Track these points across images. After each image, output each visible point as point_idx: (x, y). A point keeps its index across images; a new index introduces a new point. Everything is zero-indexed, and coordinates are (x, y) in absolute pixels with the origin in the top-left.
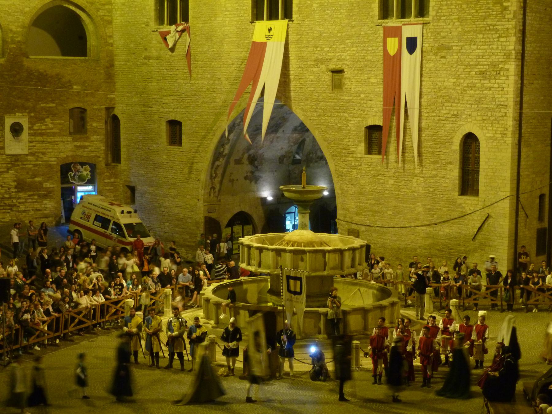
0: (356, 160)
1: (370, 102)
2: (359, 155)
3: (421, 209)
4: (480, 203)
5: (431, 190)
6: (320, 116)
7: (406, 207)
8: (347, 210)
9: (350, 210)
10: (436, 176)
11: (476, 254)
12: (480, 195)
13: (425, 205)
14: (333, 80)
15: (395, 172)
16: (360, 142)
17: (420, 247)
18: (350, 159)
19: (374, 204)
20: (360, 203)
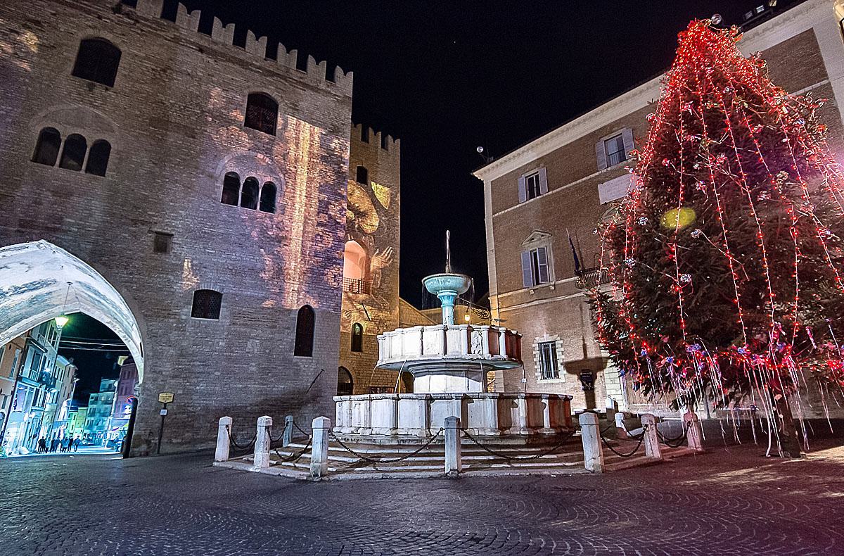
0: (179, 322)
1: (205, 269)
2: (184, 317)
3: (254, 369)
4: (314, 361)
5: (267, 351)
6: (131, 274)
7: (238, 367)
8: (160, 372)
9: (164, 373)
10: (272, 338)
11: (309, 405)
12: (313, 355)
13: (259, 365)
14: (156, 242)
15: (227, 335)
16: (188, 304)
17: (251, 404)
18: (171, 321)
19: (199, 365)
20: (179, 365)
